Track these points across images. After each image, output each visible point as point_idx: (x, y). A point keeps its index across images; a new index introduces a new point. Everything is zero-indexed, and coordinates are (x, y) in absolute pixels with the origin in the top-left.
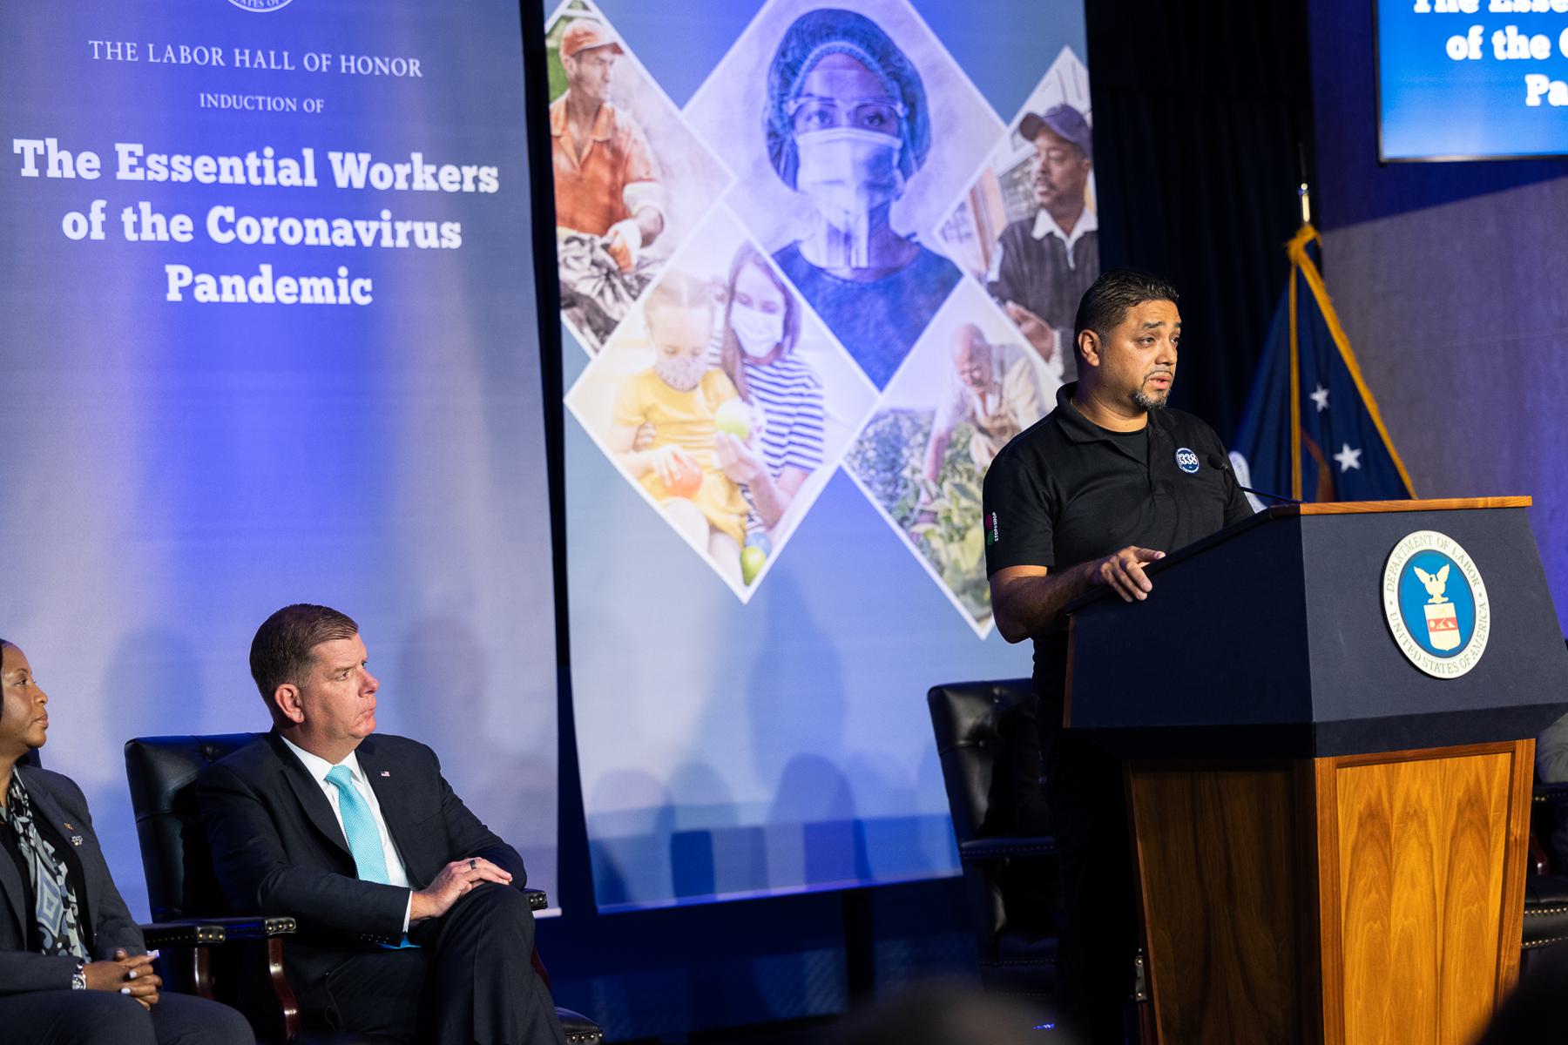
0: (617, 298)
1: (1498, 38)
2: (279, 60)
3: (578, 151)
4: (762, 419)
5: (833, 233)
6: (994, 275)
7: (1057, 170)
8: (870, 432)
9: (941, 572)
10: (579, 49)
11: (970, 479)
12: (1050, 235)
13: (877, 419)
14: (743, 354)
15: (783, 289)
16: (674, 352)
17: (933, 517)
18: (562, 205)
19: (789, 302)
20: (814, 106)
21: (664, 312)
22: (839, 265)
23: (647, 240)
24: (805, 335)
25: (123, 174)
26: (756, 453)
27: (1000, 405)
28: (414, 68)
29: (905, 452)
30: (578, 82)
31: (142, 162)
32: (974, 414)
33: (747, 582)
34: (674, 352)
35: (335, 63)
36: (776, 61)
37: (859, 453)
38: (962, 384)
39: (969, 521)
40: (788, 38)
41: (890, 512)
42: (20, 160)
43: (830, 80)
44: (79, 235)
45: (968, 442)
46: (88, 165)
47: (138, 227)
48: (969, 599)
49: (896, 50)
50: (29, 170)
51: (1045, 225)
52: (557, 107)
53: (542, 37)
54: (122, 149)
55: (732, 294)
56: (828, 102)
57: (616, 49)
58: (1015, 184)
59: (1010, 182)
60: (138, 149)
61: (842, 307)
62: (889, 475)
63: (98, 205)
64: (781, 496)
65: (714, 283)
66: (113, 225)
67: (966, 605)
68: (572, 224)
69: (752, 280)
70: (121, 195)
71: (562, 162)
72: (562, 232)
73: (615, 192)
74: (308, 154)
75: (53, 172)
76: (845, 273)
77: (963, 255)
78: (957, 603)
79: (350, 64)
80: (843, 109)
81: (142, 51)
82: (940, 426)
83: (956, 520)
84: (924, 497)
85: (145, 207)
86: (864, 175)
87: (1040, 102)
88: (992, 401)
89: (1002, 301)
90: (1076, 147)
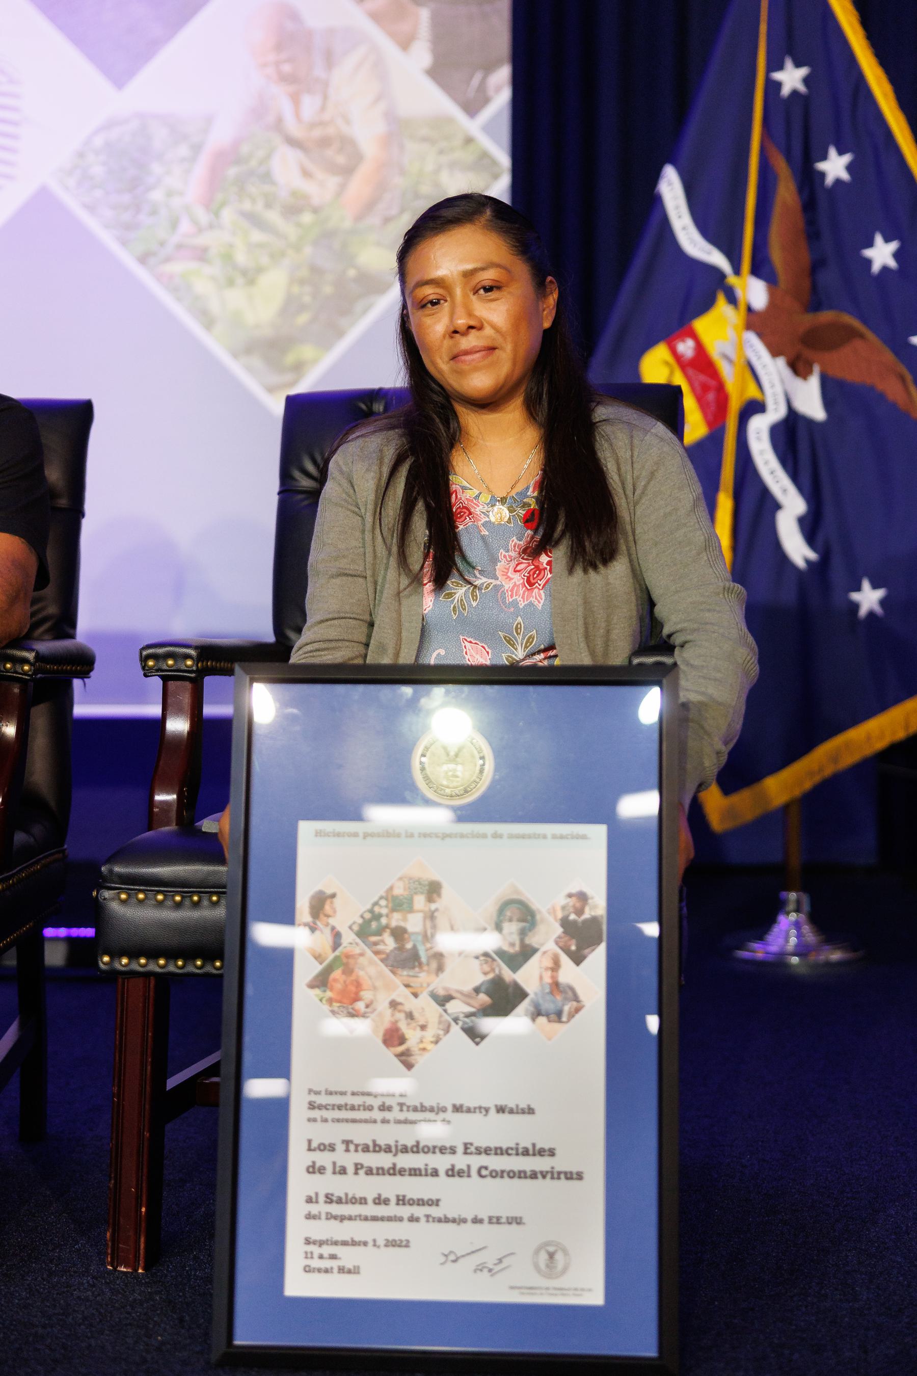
8: (98, 141)
9: (208, 322)
11: (268, 206)
13: (109, 125)
17: (202, 255)
27: (323, 108)
29: (157, 168)
32: (279, 121)
39: (265, 260)
41: (124, 243)
45: (268, 157)
48: (256, 362)
62: (126, 198)
67: (250, 369)
78: (236, 368)
82: (221, 135)
83: (241, 258)
84: (185, 226)
88: (310, 105)
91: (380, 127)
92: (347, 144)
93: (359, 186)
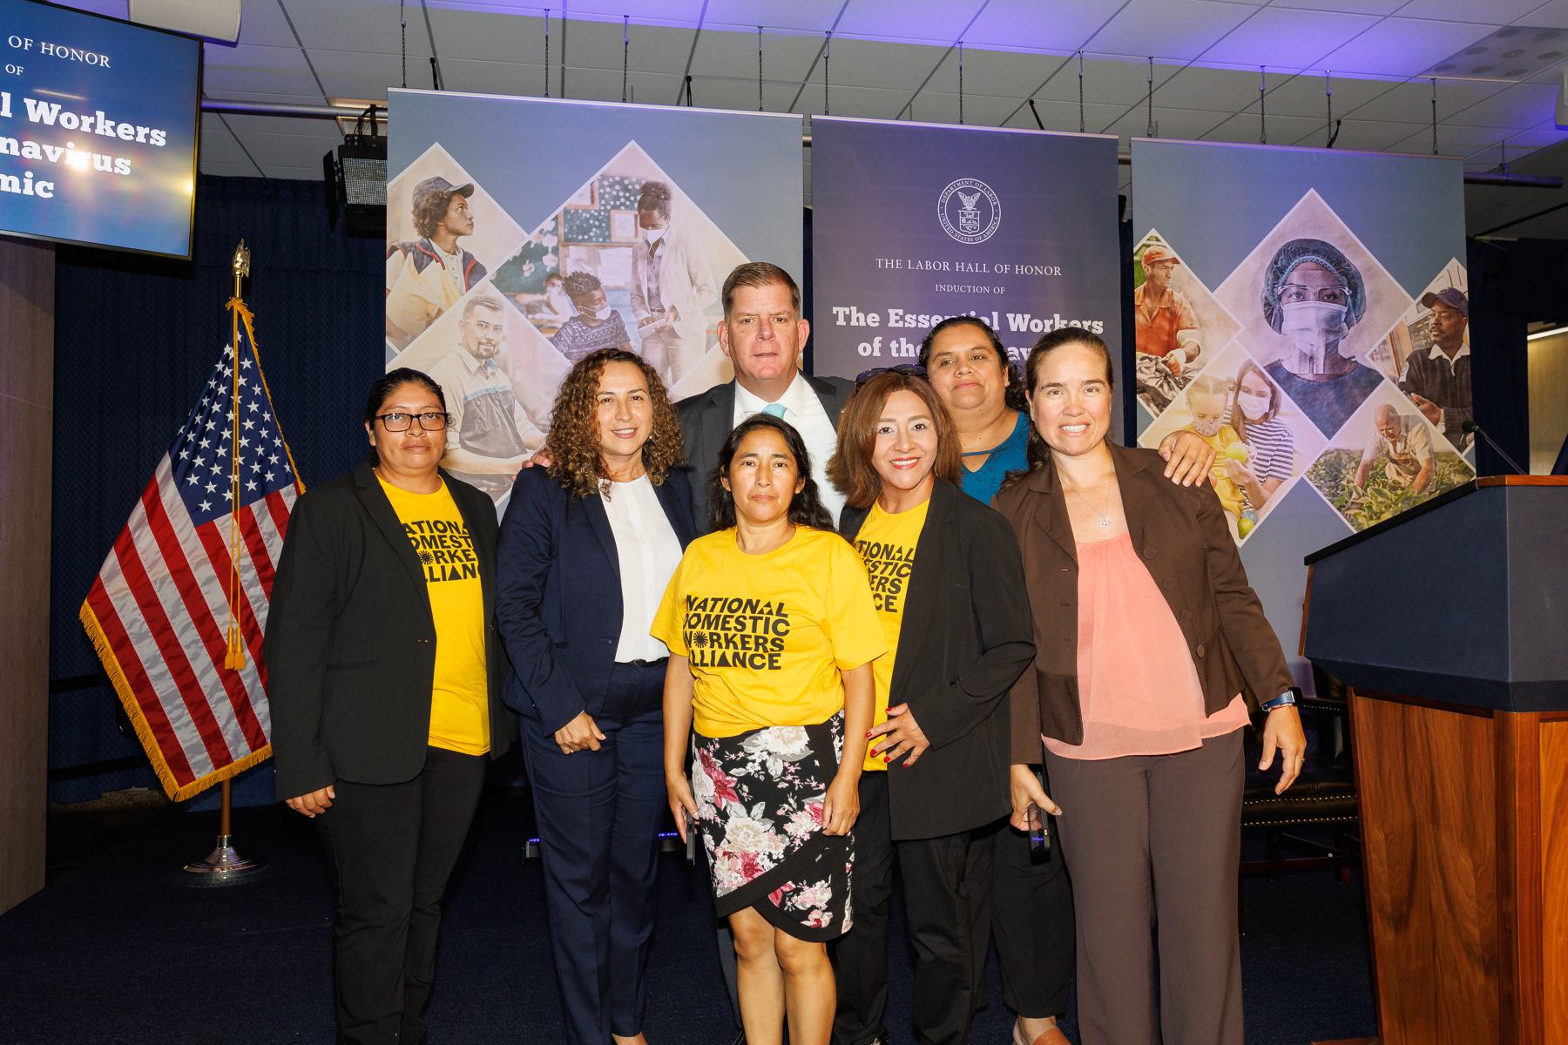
0: (1171, 388)
2: (981, 267)
3: (1150, 313)
4: (1255, 452)
5: (1303, 356)
6: (1403, 379)
7: (1445, 323)
10: (1151, 260)
12: (1440, 357)
13: (1326, 453)
14: (1244, 418)
15: (1271, 385)
16: (1203, 416)
17: (1361, 506)
18: (1139, 341)
19: (1274, 392)
20: (1294, 290)
21: (1198, 396)
22: (1305, 373)
23: (1190, 359)
24: (1283, 409)
25: (892, 324)
26: (1250, 469)
28: (1057, 271)
30: (1152, 278)
31: (902, 318)
33: (1242, 537)
34: (1203, 416)
35: (1013, 269)
36: (1271, 267)
37: (1315, 470)
38: (1379, 436)
40: (1279, 255)
42: (836, 317)
43: (1304, 276)
44: (868, 353)
46: (873, 320)
47: (899, 350)
49: (1345, 260)
50: (841, 322)
51: (1436, 352)
52: (1139, 290)
53: (1132, 255)
54: (892, 312)
55: (1238, 387)
56: (1304, 287)
57: (1175, 261)
58: (1419, 330)
59: (1415, 329)
60: (901, 312)
61: (1306, 396)
63: (877, 339)
64: (1265, 493)
65: (1229, 381)
66: (885, 349)
68: (1145, 350)
69: (1251, 379)
70: (889, 334)
71: (1140, 319)
72: (1139, 354)
73: (1172, 334)
74: (995, 314)
75: (854, 323)
76: (1310, 377)
77: (1384, 368)
79: (1021, 270)
80: (1312, 291)
81: (905, 264)
82: (1366, 458)
85: (903, 340)
86: (1323, 326)
87: (1436, 287)
88: (1400, 446)
89: (1408, 393)
90: (1458, 311)
91: (1427, 456)
92: (1415, 462)
93: (1419, 479)
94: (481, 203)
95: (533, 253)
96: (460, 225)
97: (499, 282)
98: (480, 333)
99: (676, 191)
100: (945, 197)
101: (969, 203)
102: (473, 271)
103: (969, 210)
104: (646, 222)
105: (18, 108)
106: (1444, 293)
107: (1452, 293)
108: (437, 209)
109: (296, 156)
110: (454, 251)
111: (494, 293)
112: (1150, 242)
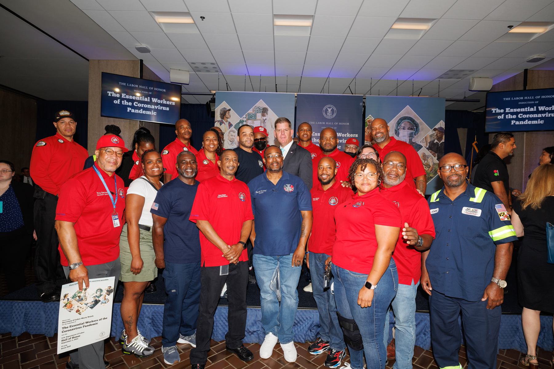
1: (507, 116)
18: (365, 139)
52: (366, 128)
59: (431, 136)
71: (366, 134)
79: (340, 124)
80: (406, 128)
94: (232, 112)
95: (241, 122)
96: (228, 117)
97: (235, 127)
98: (231, 137)
99: (269, 109)
100: (324, 109)
101: (330, 110)
102: (230, 125)
103: (330, 112)
104: (263, 115)
105: (151, 100)
106: (439, 128)
107: (441, 128)
108: (224, 114)
109: (204, 100)
110: (227, 121)
111: (234, 129)
112: (369, 118)
